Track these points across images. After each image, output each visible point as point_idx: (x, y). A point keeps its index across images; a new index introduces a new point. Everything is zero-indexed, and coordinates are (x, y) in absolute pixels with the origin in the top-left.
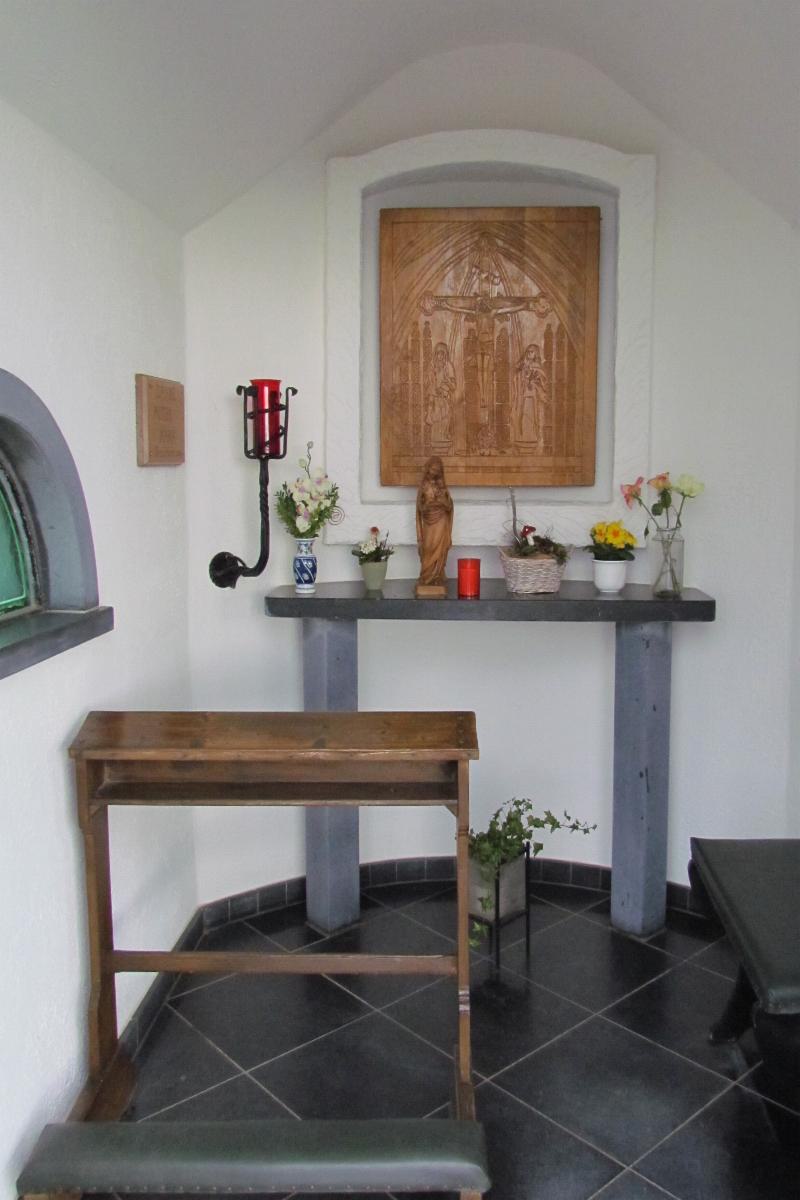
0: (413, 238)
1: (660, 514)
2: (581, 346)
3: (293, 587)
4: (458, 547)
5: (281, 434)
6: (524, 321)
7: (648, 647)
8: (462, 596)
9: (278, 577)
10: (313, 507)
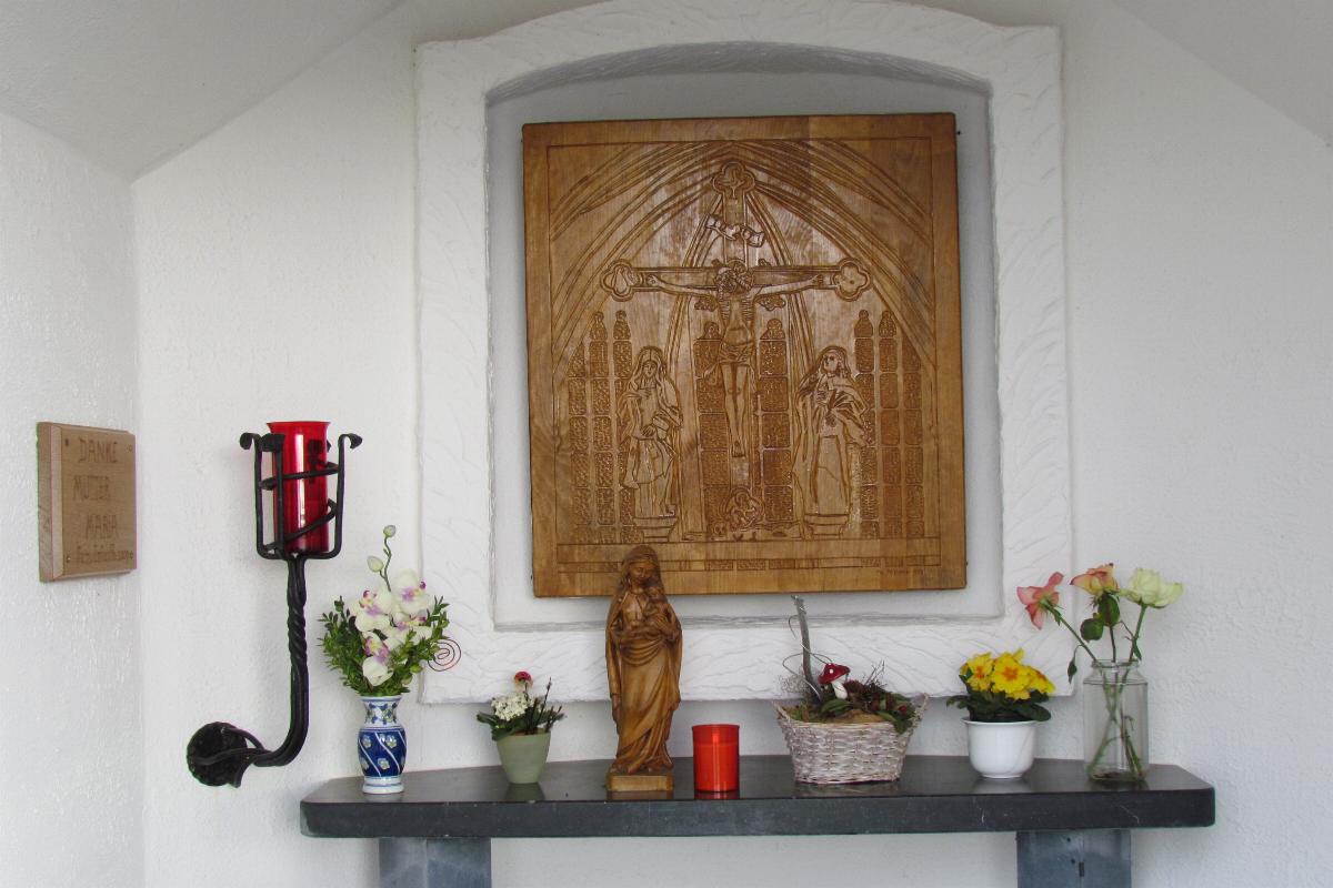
0: (588, 172)
1: (1097, 638)
2: (928, 347)
3: (358, 782)
4: (687, 702)
5: (330, 517)
6: (814, 307)
7: (1082, 874)
8: (702, 793)
9: (328, 761)
10: (395, 640)
